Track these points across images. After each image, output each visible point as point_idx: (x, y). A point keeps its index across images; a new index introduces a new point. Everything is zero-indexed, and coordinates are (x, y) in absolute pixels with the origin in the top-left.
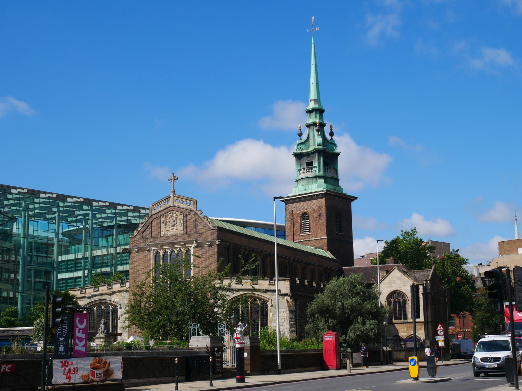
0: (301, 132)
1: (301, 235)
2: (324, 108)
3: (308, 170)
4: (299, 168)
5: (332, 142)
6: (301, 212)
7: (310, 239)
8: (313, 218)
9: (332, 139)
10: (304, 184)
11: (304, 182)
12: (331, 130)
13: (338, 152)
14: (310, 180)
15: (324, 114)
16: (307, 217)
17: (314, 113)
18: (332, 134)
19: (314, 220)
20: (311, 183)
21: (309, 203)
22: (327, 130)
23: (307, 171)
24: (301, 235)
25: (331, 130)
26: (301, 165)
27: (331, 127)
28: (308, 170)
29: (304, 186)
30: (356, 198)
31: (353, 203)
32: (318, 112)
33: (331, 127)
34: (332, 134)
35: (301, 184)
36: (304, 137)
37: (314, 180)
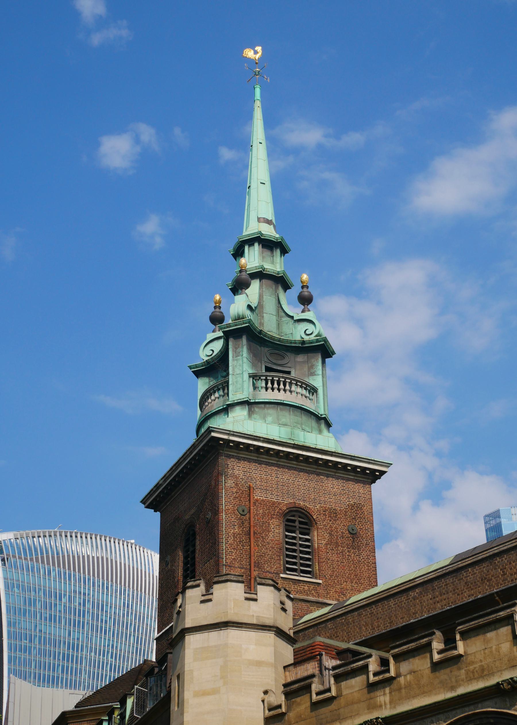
1: (282, 575)
3: (290, 387)
4: (251, 372)
6: (287, 501)
7: (320, 600)
8: (330, 534)
10: (283, 420)
11: (287, 416)
14: (304, 418)
16: (300, 523)
19: (333, 543)
20: (307, 429)
21: (312, 485)
24: (282, 575)
26: (254, 365)
28: (290, 387)
29: (288, 429)
35: (269, 419)
37: (313, 423)
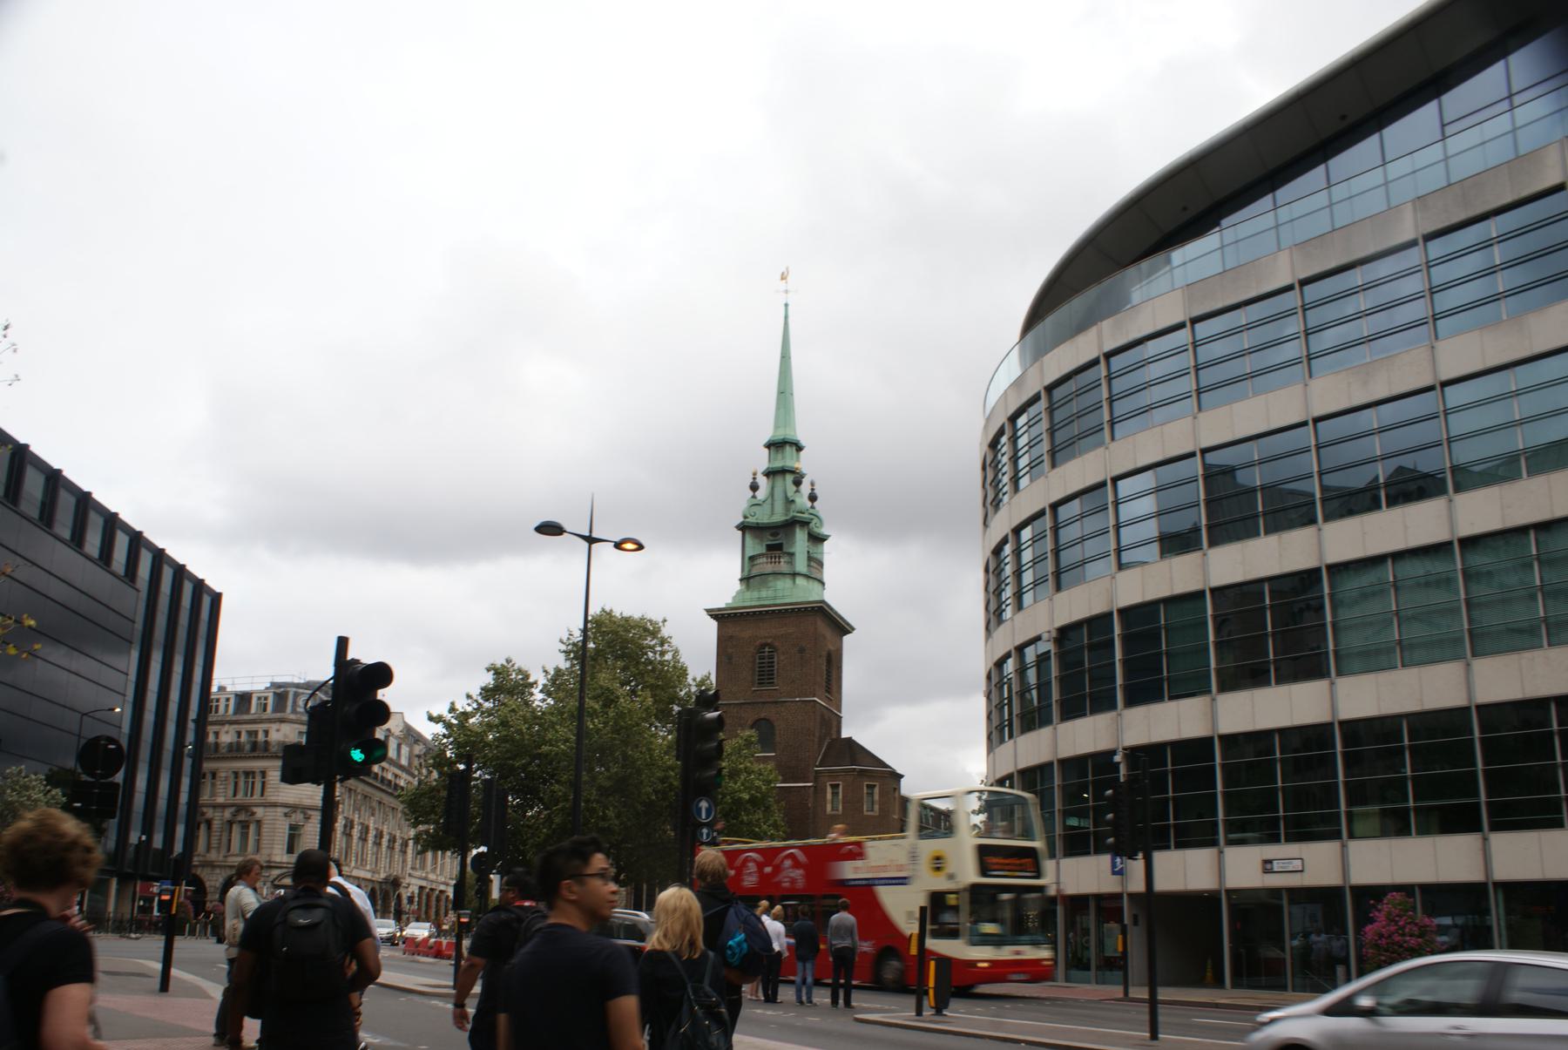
0: (756, 483)
2: (803, 443)
5: (811, 511)
9: (812, 507)
12: (813, 489)
13: (826, 533)
15: (802, 453)
17: (788, 448)
18: (813, 498)
22: (805, 488)
23: (777, 560)
25: (813, 489)
27: (812, 484)
30: (853, 629)
31: (846, 638)
32: (794, 448)
33: (812, 484)
34: (813, 498)
36: (762, 494)
